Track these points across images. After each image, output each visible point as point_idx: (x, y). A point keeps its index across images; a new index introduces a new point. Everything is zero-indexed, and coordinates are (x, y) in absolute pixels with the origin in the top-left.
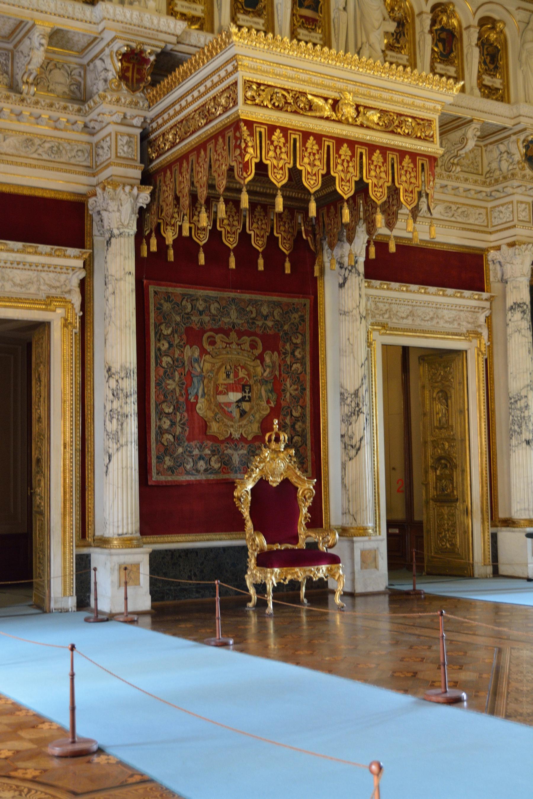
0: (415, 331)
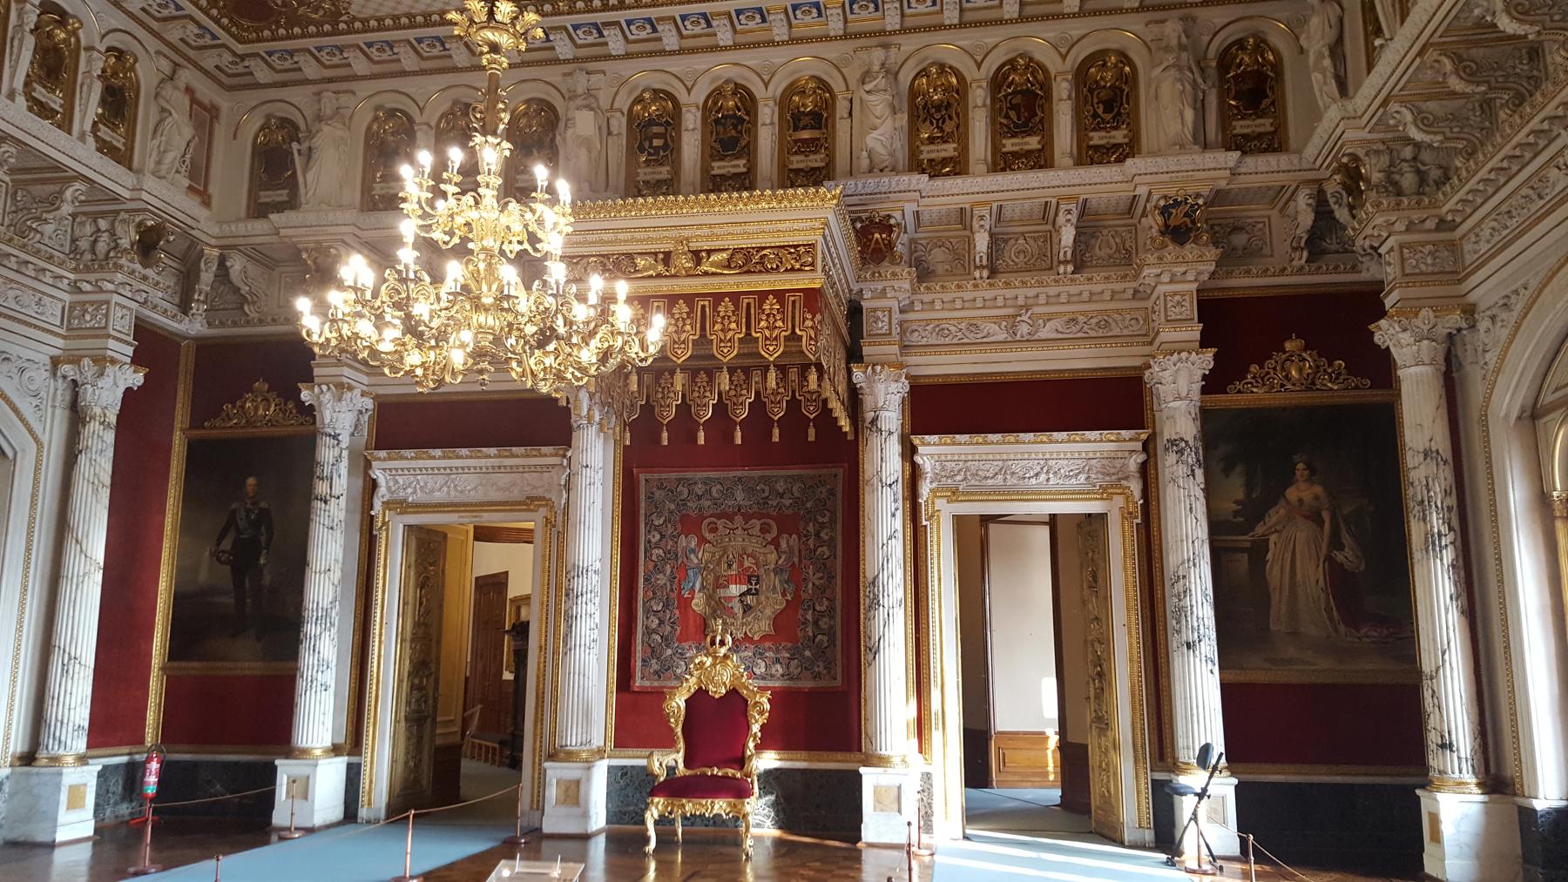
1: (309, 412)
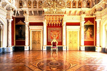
1: (25, 23)
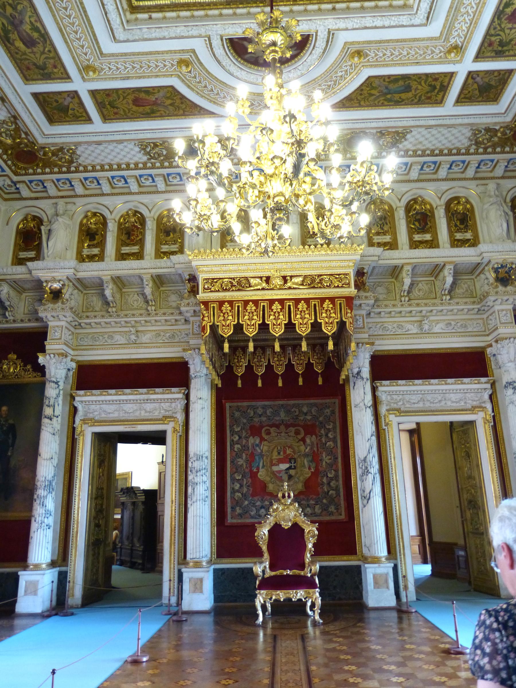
0: (426, 411)
1: (41, 370)
